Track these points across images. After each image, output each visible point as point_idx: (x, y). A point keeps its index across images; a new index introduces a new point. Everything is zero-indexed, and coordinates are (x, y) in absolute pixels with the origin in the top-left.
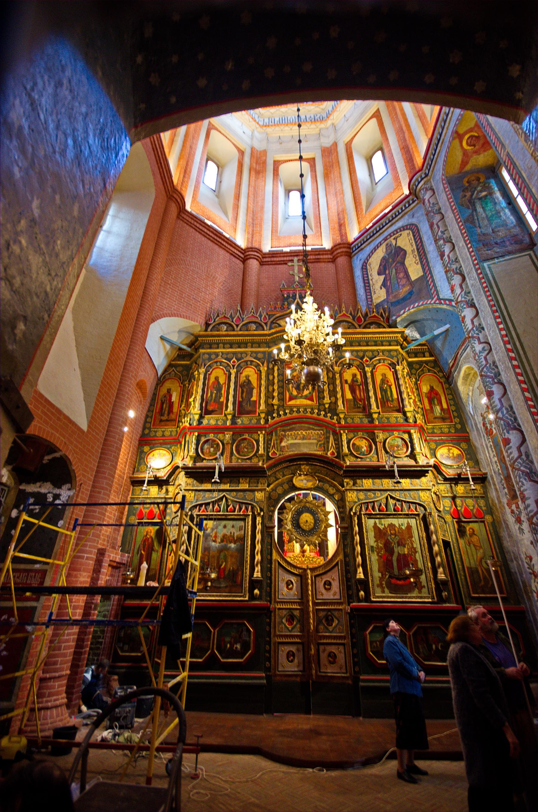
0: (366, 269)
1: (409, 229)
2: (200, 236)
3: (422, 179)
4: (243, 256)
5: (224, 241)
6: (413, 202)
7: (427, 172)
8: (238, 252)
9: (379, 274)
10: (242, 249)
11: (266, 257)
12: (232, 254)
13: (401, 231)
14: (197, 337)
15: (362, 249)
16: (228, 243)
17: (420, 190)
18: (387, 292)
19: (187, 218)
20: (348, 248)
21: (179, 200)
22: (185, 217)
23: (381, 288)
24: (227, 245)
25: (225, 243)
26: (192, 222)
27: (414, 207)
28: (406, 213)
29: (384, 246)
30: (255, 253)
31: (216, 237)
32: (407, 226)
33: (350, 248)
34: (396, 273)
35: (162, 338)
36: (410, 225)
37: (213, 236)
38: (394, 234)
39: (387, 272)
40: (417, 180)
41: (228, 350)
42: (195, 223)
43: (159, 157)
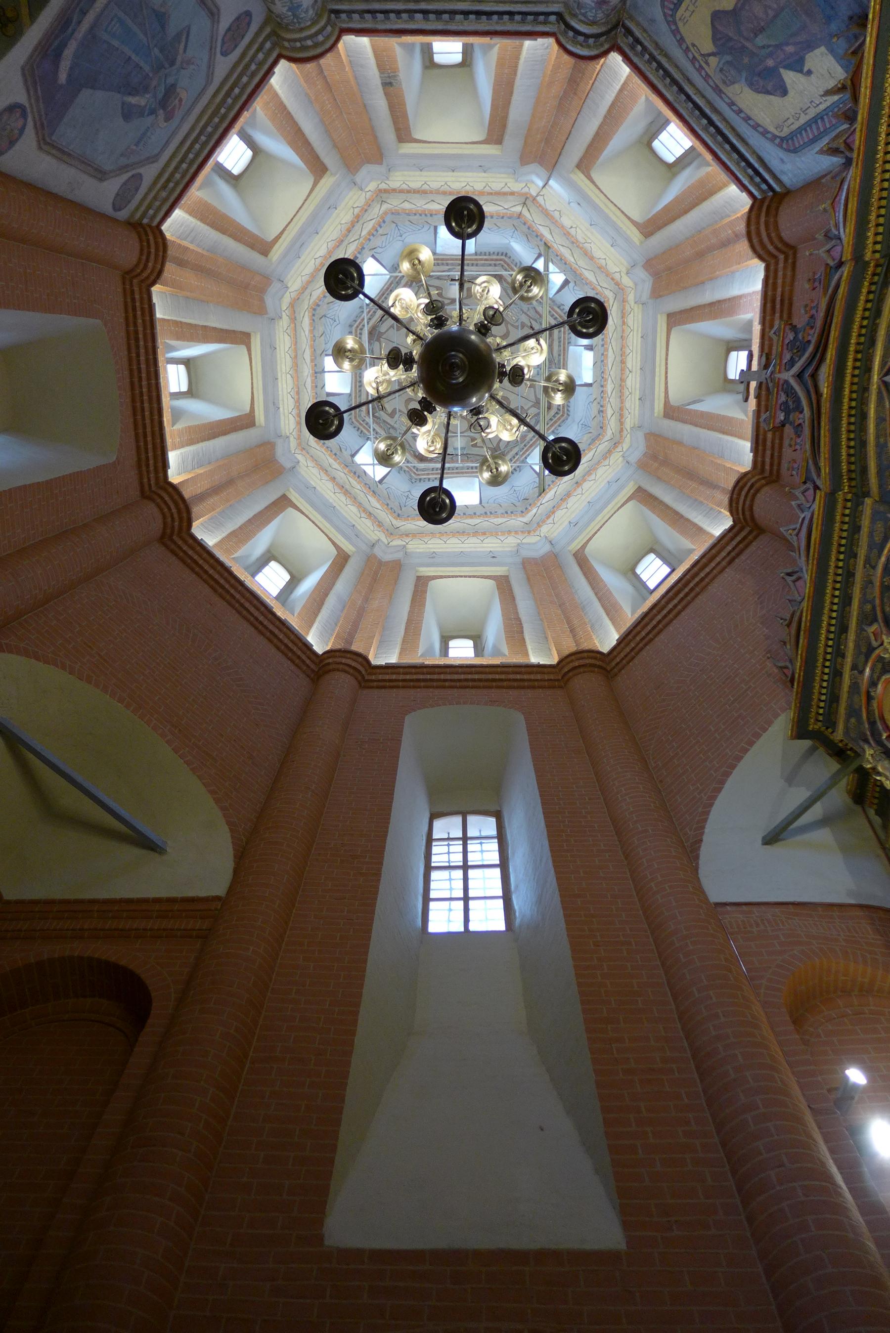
0: (792, 136)
1: (675, 23)
2: (662, 636)
3: (569, 27)
4: (748, 529)
5: (697, 574)
6: (629, 32)
7: (553, 18)
8: (734, 543)
9: (783, 91)
10: (731, 529)
11: (763, 463)
12: (730, 563)
13: (687, 48)
14: (801, 731)
15: (761, 160)
16: (705, 566)
17: (593, 23)
18: (810, 46)
19: (622, 655)
20: (760, 209)
21: (577, 664)
22: (618, 660)
23: (809, 73)
24: (707, 570)
25: (702, 575)
26: (633, 645)
27: (638, 24)
28: (657, 46)
29: (731, 91)
30: (743, 493)
31: (681, 595)
32: (673, 32)
33: (763, 201)
34: (762, 30)
35: (772, 839)
36: (668, 23)
37: (675, 601)
38: (701, 66)
39: (770, 63)
40: (575, 42)
41: (851, 645)
42: (638, 638)
43: (480, 680)
